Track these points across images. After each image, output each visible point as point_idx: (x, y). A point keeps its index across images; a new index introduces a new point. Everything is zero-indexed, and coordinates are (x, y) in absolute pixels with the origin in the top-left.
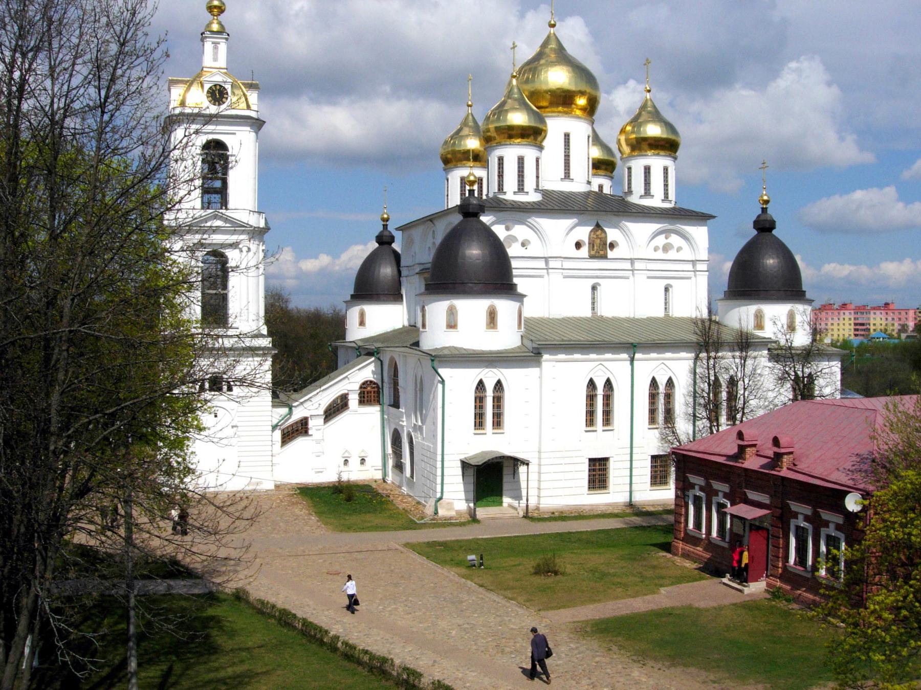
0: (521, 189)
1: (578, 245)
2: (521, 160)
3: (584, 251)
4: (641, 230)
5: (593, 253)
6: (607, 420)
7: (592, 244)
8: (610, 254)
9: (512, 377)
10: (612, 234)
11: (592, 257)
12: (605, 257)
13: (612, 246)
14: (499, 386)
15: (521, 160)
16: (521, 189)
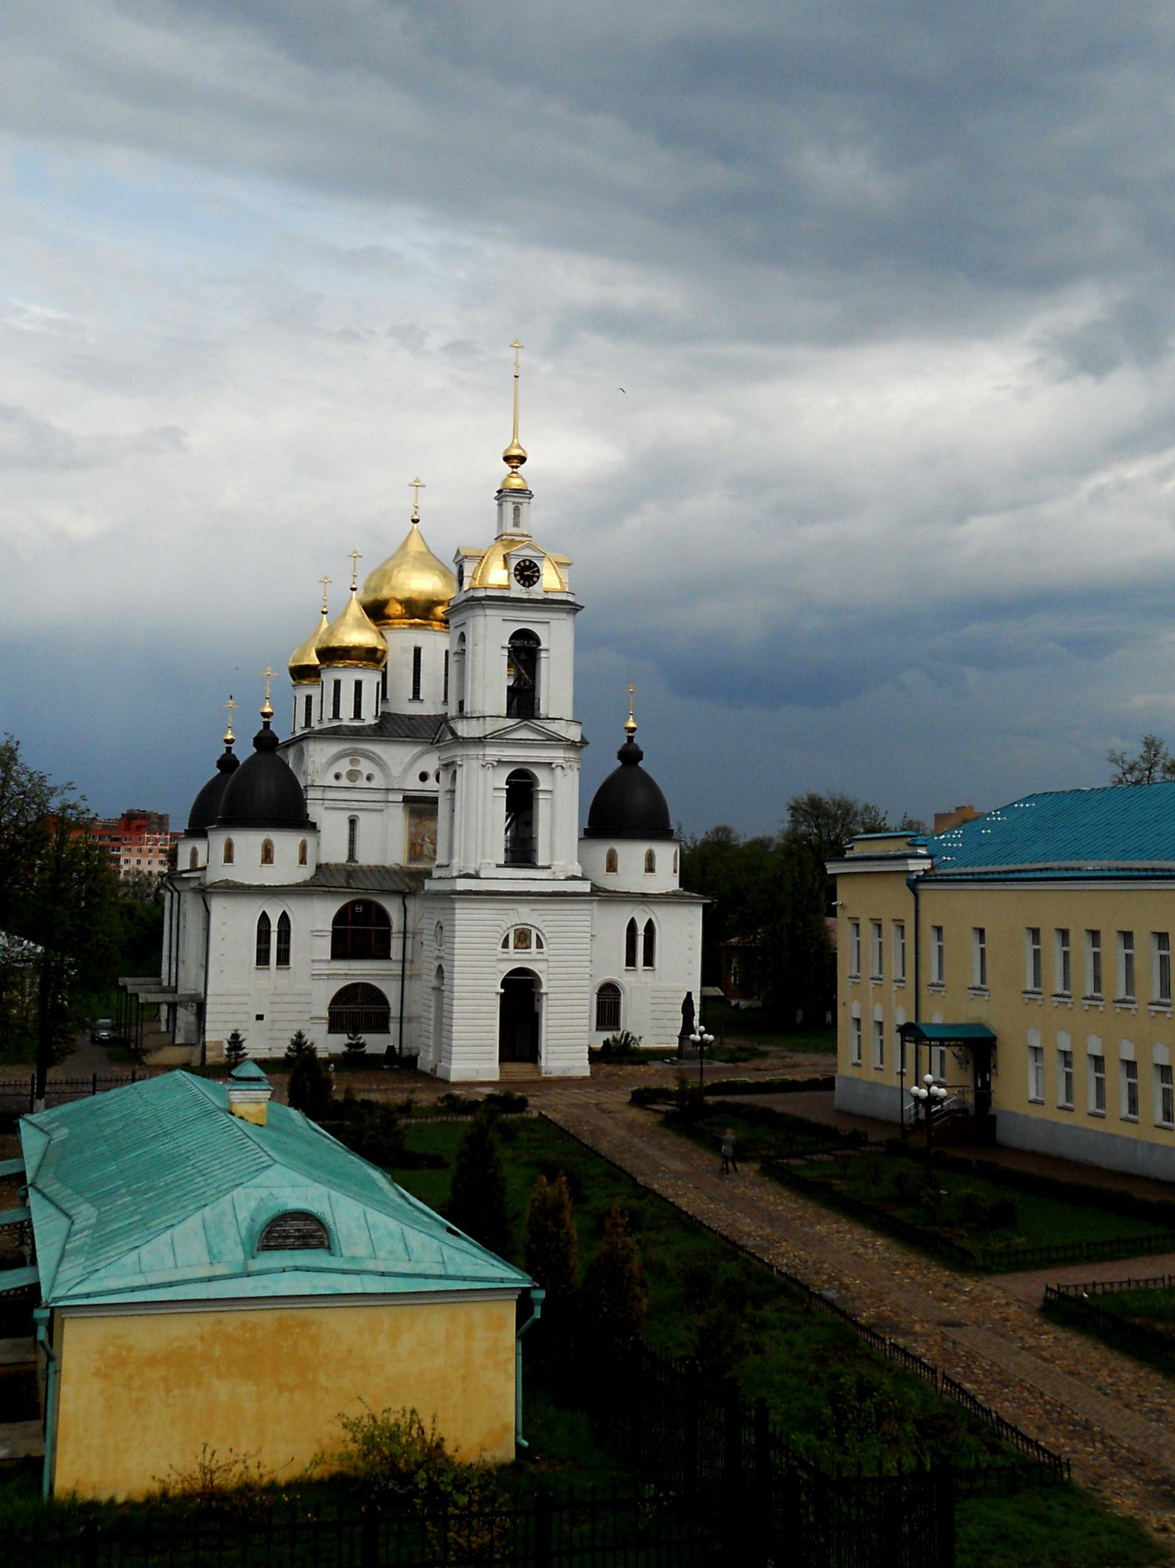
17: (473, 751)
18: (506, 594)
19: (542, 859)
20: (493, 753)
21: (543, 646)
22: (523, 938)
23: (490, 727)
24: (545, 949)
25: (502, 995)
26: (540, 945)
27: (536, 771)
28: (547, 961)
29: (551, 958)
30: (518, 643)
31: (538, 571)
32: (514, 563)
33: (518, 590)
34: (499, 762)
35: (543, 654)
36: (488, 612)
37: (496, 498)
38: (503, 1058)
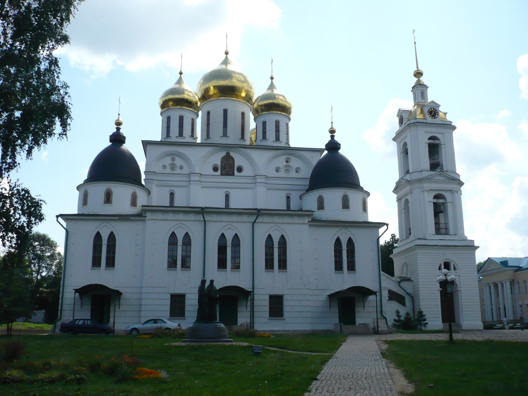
0: (181, 134)
1: (215, 169)
2: (181, 118)
3: (219, 173)
4: (260, 158)
5: (224, 172)
6: (186, 265)
7: (223, 167)
8: (236, 173)
9: (122, 231)
10: (239, 160)
11: (222, 174)
12: (233, 174)
13: (240, 170)
14: (112, 237)
15: (181, 118)
16: (181, 134)
17: (416, 185)
18: (424, 121)
19: (451, 231)
20: (427, 186)
21: (442, 142)
22: (447, 266)
23: (425, 174)
24: (457, 271)
25: (441, 292)
26: (455, 269)
27: (445, 194)
28: (459, 276)
29: (461, 275)
30: (431, 141)
31: (437, 113)
32: (426, 110)
33: (429, 119)
34: (430, 190)
35: (443, 146)
36: (419, 128)
37: (412, 91)
38: (443, 322)
